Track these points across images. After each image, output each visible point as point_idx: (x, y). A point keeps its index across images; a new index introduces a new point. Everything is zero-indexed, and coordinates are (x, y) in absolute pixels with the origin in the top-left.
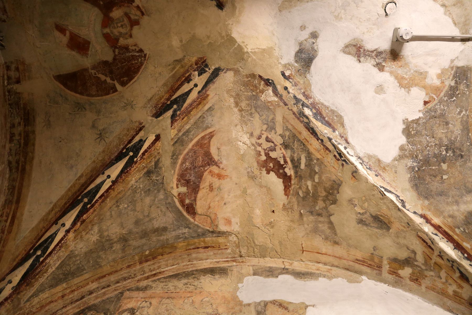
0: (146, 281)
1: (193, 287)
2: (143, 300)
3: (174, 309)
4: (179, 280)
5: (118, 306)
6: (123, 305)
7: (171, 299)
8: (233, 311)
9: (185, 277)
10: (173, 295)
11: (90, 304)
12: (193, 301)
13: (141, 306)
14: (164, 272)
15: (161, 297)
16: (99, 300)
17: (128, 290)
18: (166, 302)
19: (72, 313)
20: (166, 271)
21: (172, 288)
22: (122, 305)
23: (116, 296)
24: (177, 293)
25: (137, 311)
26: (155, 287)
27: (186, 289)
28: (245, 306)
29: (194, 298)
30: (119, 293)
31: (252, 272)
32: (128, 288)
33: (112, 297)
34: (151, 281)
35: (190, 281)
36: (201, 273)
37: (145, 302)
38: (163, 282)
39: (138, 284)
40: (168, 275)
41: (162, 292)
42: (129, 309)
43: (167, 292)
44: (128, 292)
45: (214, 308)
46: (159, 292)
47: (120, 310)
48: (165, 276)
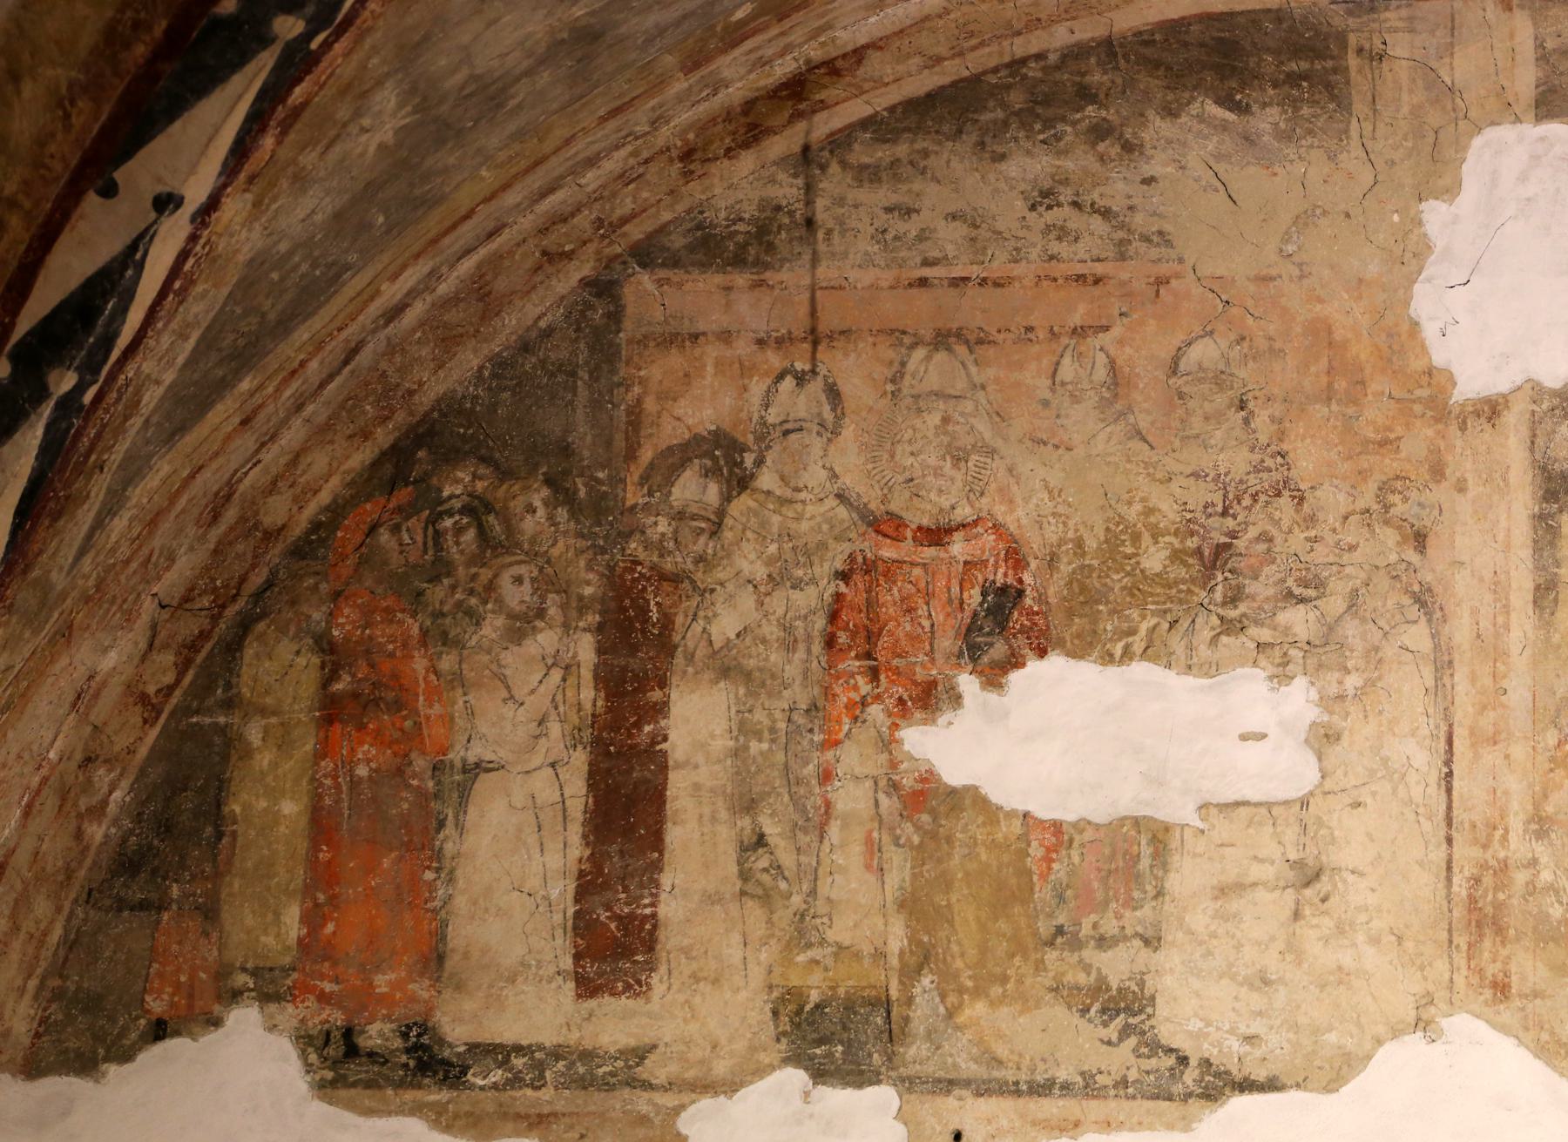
0: (747, 162)
1: (1097, 223)
2: (775, 360)
3: (998, 443)
4: (990, 151)
5: (621, 414)
6: (650, 405)
7: (961, 350)
8: (1389, 465)
9: (1026, 117)
10: (971, 309)
11: (424, 401)
12: (1112, 363)
13: (773, 416)
14: (858, 54)
15: (894, 333)
16: (469, 359)
17: (645, 254)
18: (933, 381)
19: (335, 481)
20: (874, 45)
21: (950, 237)
22: (639, 401)
23: (577, 316)
24: (997, 284)
25: (759, 462)
26: (829, 232)
27: (1055, 247)
28: (1463, 428)
29: (1121, 342)
30: (585, 283)
31: (1525, 80)
32: (636, 231)
33: (548, 333)
34: (781, 162)
35: (1069, 164)
36: (1145, 81)
37: (788, 383)
38: (869, 175)
39: (695, 191)
40: (894, 95)
41: (887, 278)
42: (697, 439)
43: (923, 282)
44: (646, 280)
45: (1263, 439)
46: (866, 277)
47: (646, 455)
48: (882, 101)
